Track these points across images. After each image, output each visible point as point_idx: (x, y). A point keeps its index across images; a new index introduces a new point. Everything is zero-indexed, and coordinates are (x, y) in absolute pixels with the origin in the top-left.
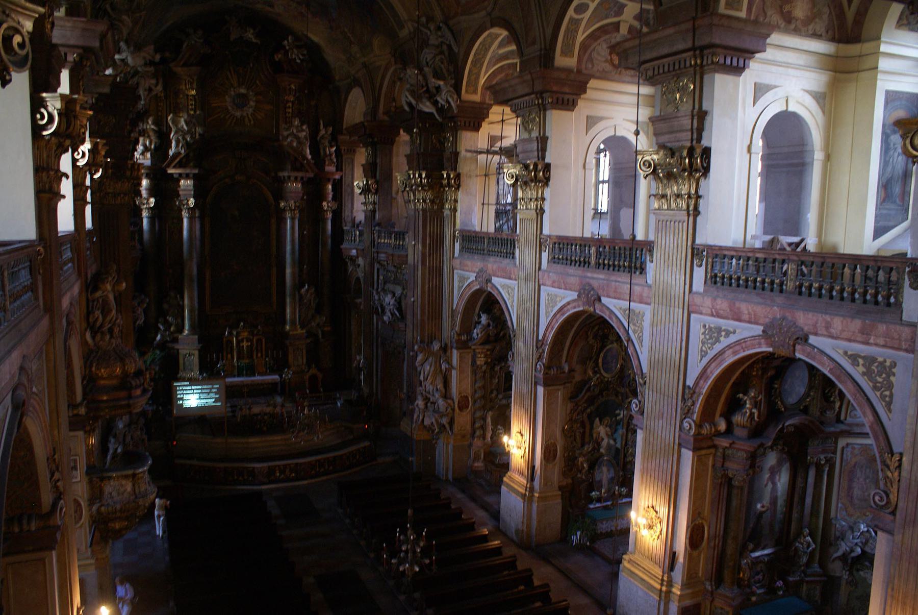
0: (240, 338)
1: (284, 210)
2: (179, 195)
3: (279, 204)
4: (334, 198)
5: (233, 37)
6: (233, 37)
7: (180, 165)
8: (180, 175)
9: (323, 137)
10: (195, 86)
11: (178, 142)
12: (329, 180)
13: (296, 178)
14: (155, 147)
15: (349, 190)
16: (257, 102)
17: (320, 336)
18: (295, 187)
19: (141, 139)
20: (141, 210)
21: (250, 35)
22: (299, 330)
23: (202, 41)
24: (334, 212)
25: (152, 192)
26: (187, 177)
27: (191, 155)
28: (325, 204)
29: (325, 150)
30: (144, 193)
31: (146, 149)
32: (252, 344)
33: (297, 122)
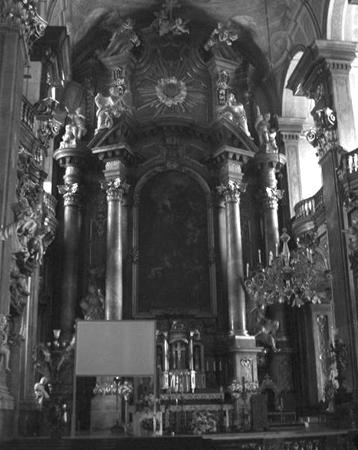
0: (172, 341)
1: (222, 197)
2: (104, 178)
3: (216, 191)
4: (279, 187)
5: (161, 33)
6: (161, 33)
7: (106, 143)
8: (105, 153)
9: (261, 123)
10: (123, 75)
11: (104, 117)
12: (271, 165)
13: (234, 158)
14: (82, 135)
15: (295, 180)
16: (188, 91)
17: (274, 345)
18: (234, 169)
19: (67, 127)
20: (63, 200)
21: (179, 27)
22: (245, 332)
23: (131, 28)
24: (279, 202)
25: (75, 178)
26: (112, 156)
27: (119, 133)
28: (268, 190)
29: (264, 137)
30: (67, 179)
31: (72, 137)
32: (188, 350)
33: (232, 98)
